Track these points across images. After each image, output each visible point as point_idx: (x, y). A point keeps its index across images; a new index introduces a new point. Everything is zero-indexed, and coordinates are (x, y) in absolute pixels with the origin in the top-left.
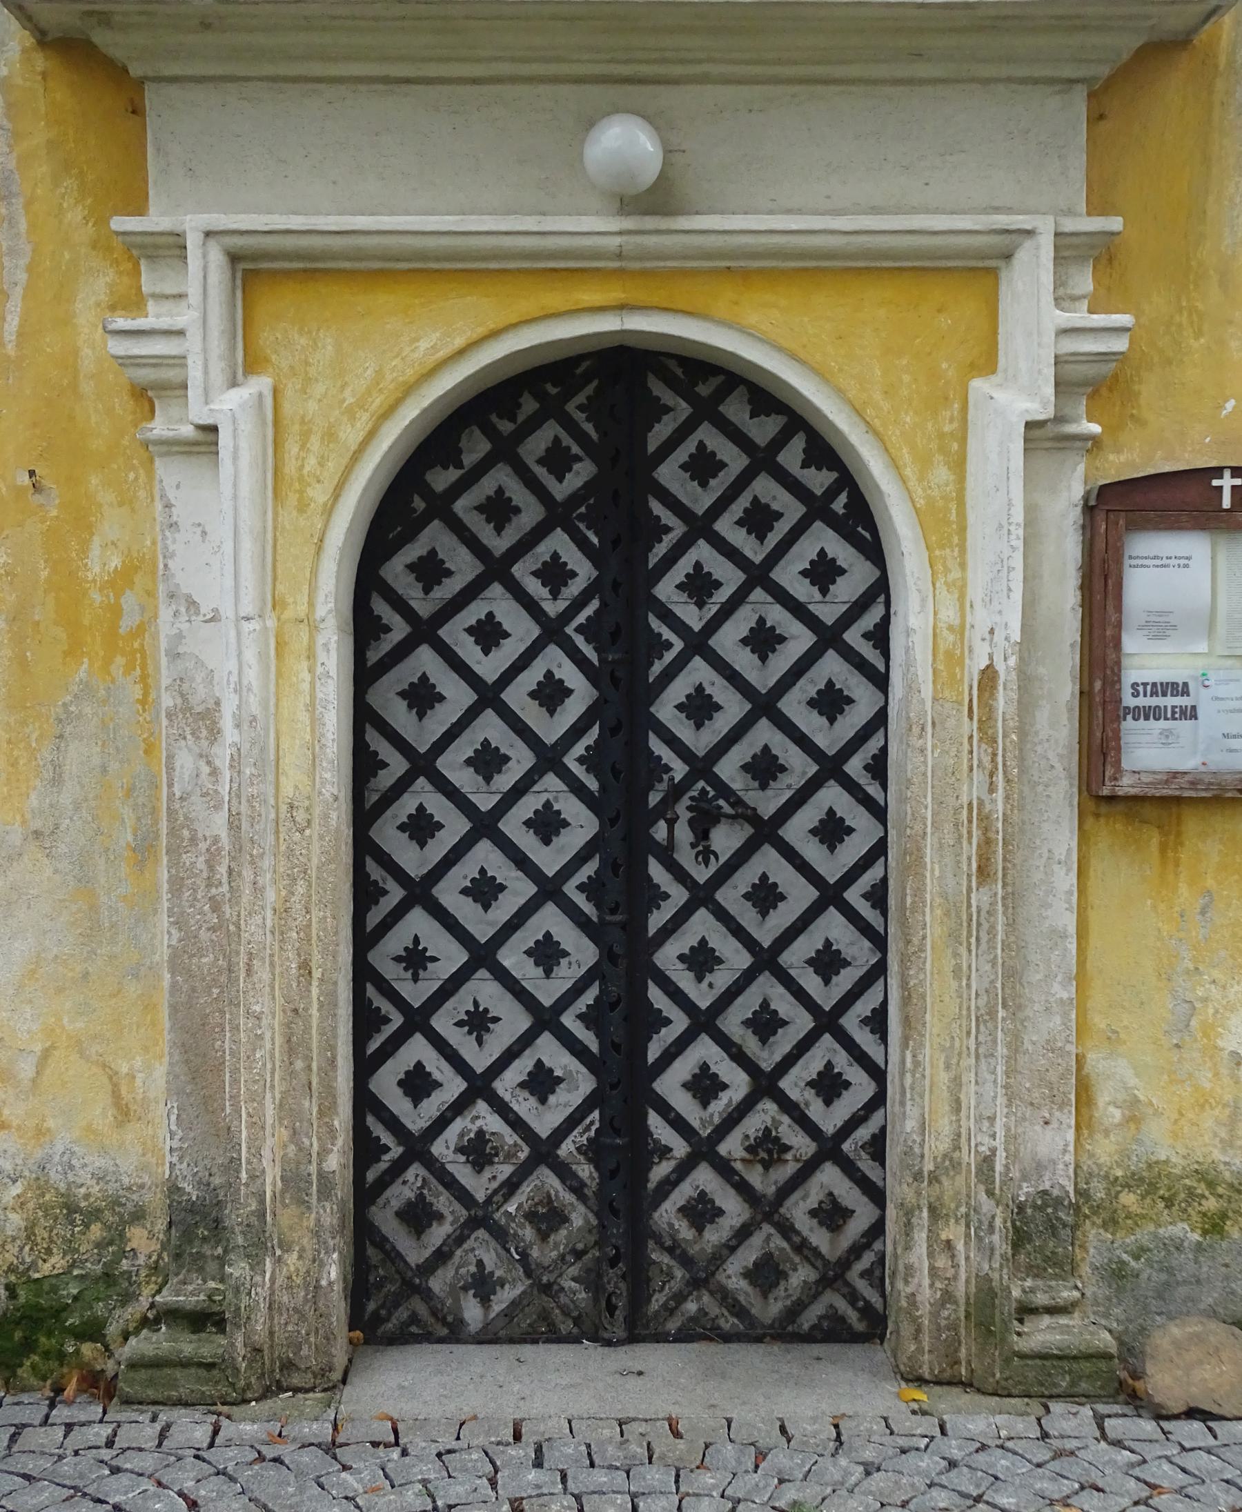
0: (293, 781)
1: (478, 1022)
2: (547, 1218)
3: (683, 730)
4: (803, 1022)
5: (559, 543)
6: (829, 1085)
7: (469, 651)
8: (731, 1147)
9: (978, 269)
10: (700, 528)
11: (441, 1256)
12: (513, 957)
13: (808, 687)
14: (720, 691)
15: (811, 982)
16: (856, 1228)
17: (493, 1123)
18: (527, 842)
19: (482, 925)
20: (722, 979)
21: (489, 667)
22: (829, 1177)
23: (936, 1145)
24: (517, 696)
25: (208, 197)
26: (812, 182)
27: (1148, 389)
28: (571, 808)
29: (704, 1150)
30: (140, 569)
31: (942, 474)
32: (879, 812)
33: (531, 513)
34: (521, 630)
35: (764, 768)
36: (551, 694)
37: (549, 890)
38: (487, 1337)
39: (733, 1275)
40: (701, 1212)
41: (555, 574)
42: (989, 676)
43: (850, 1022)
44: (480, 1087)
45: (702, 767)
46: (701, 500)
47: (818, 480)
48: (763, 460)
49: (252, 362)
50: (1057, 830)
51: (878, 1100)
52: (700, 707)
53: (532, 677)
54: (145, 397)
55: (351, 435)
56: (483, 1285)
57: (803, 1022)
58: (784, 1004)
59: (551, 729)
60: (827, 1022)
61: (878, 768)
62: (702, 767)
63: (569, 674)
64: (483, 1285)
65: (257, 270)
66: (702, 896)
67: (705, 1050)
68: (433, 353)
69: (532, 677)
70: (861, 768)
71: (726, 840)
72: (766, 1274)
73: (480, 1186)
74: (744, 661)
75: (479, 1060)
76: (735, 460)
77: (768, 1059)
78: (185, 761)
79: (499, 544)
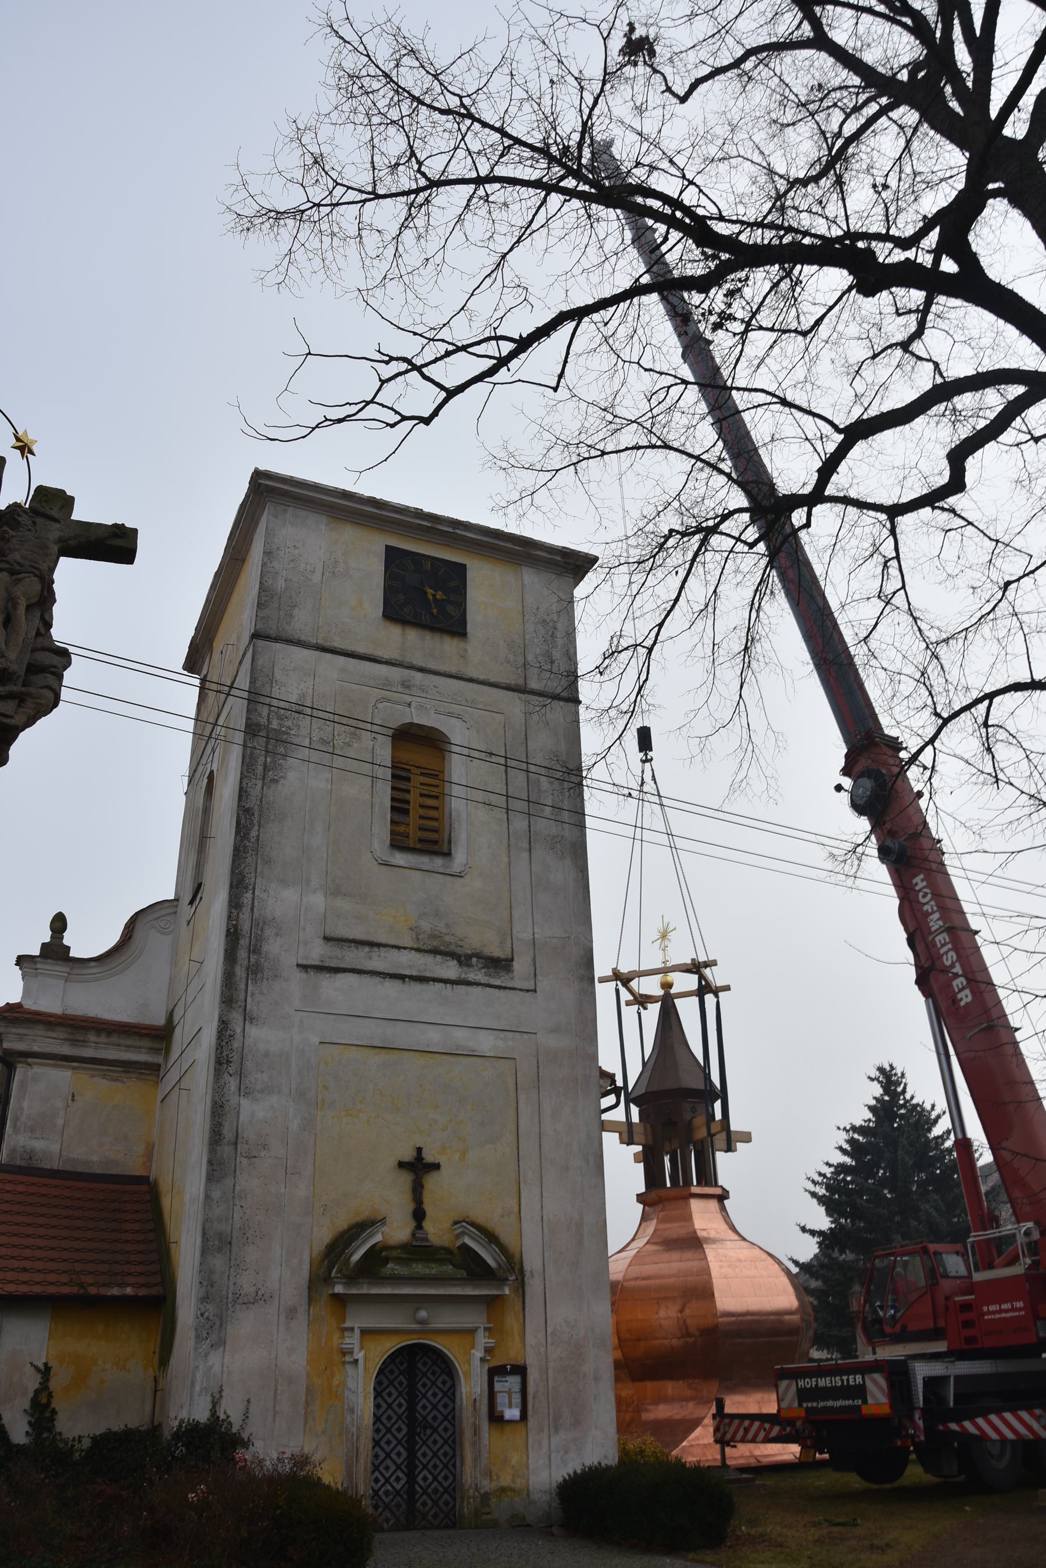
2: (398, 1506)
3: (421, 1411)
4: (441, 1466)
5: (401, 1378)
6: (446, 1478)
7: (386, 1397)
8: (429, 1490)
9: (472, 1332)
10: (424, 1375)
11: (380, 1514)
12: (393, 1456)
14: (427, 1404)
15: (443, 1458)
16: (451, 1505)
17: (389, 1488)
18: (396, 1433)
19: (388, 1449)
20: (428, 1458)
22: (446, 1496)
24: (394, 1406)
25: (358, 1320)
26: (447, 1319)
28: (403, 1427)
29: (425, 1492)
31: (467, 1366)
32: (454, 1426)
33: (397, 1372)
34: (395, 1394)
35: (435, 1418)
36: (400, 1405)
40: (424, 1504)
41: (401, 1383)
42: (475, 1400)
43: (449, 1466)
44: (387, 1481)
46: (424, 1370)
47: (443, 1366)
49: (362, 1348)
51: (454, 1480)
52: (424, 1407)
53: (397, 1402)
54: (344, 1354)
55: (377, 1360)
56: (387, 1520)
58: (438, 1463)
60: (445, 1466)
61: (454, 1418)
62: (425, 1418)
63: (403, 1402)
64: (387, 1520)
65: (365, 1332)
66: (425, 1443)
68: (390, 1345)
69: (397, 1402)
70: (452, 1417)
71: (429, 1432)
72: (435, 1516)
73: (386, 1500)
76: (430, 1363)
77: (436, 1473)
78: (349, 1418)
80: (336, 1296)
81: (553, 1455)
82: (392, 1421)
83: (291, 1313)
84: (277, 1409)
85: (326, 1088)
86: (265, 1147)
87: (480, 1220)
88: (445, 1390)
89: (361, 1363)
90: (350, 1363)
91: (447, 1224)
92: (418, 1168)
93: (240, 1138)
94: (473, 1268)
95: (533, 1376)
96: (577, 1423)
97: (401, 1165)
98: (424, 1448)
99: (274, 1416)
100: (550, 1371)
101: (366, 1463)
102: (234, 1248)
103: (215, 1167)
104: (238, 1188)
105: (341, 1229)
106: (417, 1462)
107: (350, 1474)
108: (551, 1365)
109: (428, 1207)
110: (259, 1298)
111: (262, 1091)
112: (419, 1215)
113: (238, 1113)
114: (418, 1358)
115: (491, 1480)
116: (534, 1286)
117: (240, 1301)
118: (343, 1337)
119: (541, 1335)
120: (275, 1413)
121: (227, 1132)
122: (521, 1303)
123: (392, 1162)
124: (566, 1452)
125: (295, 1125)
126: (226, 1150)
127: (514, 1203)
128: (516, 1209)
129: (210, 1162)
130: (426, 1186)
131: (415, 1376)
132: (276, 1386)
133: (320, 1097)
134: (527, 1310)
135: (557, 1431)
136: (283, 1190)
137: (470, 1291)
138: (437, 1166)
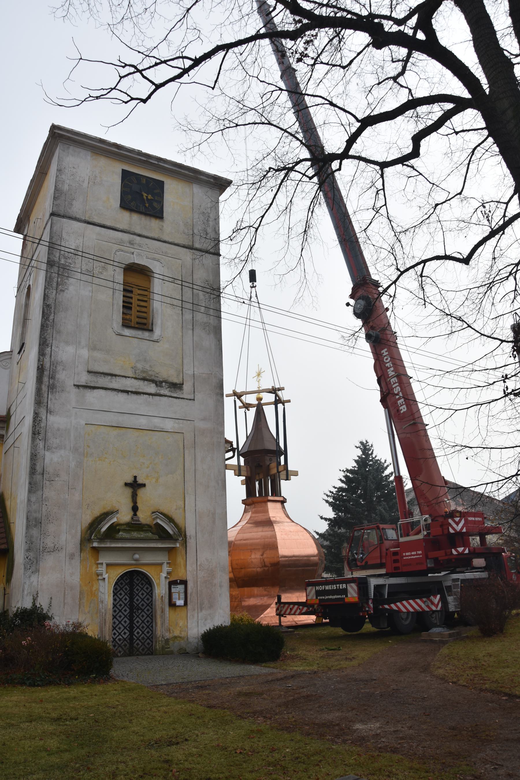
0: (109, 607)
1: (120, 628)
2: (125, 645)
5: (126, 586)
6: (148, 632)
7: (119, 596)
8: (140, 638)
9: (161, 564)
10: (138, 585)
11: (117, 649)
12: (122, 622)
13: (146, 598)
14: (139, 599)
15: (146, 623)
16: (150, 645)
17: (121, 637)
18: (124, 612)
19: (120, 619)
20: (139, 623)
21: (121, 597)
22: (148, 641)
23: (159, 635)
24: (123, 600)
25: (105, 559)
26: (149, 558)
27: (173, 573)
28: (127, 609)
30: (98, 589)
32: (152, 608)
33: (124, 584)
34: (123, 594)
35: (143, 605)
36: (126, 599)
37: (125, 616)
38: (121, 656)
39: (140, 650)
40: (138, 644)
41: (126, 589)
42: (162, 596)
44: (120, 634)
45: (138, 605)
46: (138, 583)
47: (147, 581)
48: (142, 579)
49: (107, 573)
50: (167, 608)
51: (152, 633)
52: (137, 600)
53: (124, 598)
54: (98, 575)
55: (114, 578)
56: (120, 652)
57: (146, 627)
58: (144, 626)
59: (126, 602)
60: (148, 627)
61: (152, 605)
62: (138, 605)
63: (127, 597)
64: (120, 652)
65: (108, 565)
66: (138, 616)
67: (138, 630)
68: (121, 571)
69: (124, 598)
70: (151, 605)
71: (140, 611)
72: (143, 650)
73: (120, 643)
74: (141, 596)
75: (120, 632)
79: (122, 586)
80: (94, 548)
81: (199, 621)
82: (122, 607)
83: (72, 556)
84: (66, 601)
85: (88, 446)
86: (58, 475)
87: (165, 511)
88: (148, 592)
89: (106, 580)
90: (101, 579)
91: (149, 513)
92: (135, 486)
93: (45, 471)
94: (161, 534)
95: (190, 585)
96: (211, 607)
97: (126, 484)
98: (138, 619)
99: (64, 605)
100: (198, 583)
101: (109, 626)
102: (43, 525)
103: (32, 486)
104: (44, 496)
105: (96, 516)
106: (134, 625)
107: (101, 631)
108: (199, 580)
109: (139, 505)
110: (55, 549)
111: (56, 448)
112: (135, 509)
113: (44, 459)
114: (134, 577)
115: (170, 633)
116: (191, 543)
117: (46, 551)
118: (98, 567)
119: (195, 566)
120: (64, 604)
121: (39, 468)
122: (185, 551)
123: (122, 483)
124: (206, 620)
125: (73, 464)
126: (38, 477)
127: (182, 503)
128: (183, 506)
129: (30, 483)
130: (138, 495)
131: (133, 586)
132: (65, 591)
133: (85, 451)
134: (188, 554)
135: (201, 610)
136: (67, 497)
137: (160, 545)
138: (144, 485)
